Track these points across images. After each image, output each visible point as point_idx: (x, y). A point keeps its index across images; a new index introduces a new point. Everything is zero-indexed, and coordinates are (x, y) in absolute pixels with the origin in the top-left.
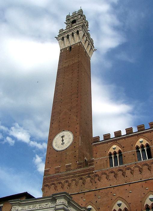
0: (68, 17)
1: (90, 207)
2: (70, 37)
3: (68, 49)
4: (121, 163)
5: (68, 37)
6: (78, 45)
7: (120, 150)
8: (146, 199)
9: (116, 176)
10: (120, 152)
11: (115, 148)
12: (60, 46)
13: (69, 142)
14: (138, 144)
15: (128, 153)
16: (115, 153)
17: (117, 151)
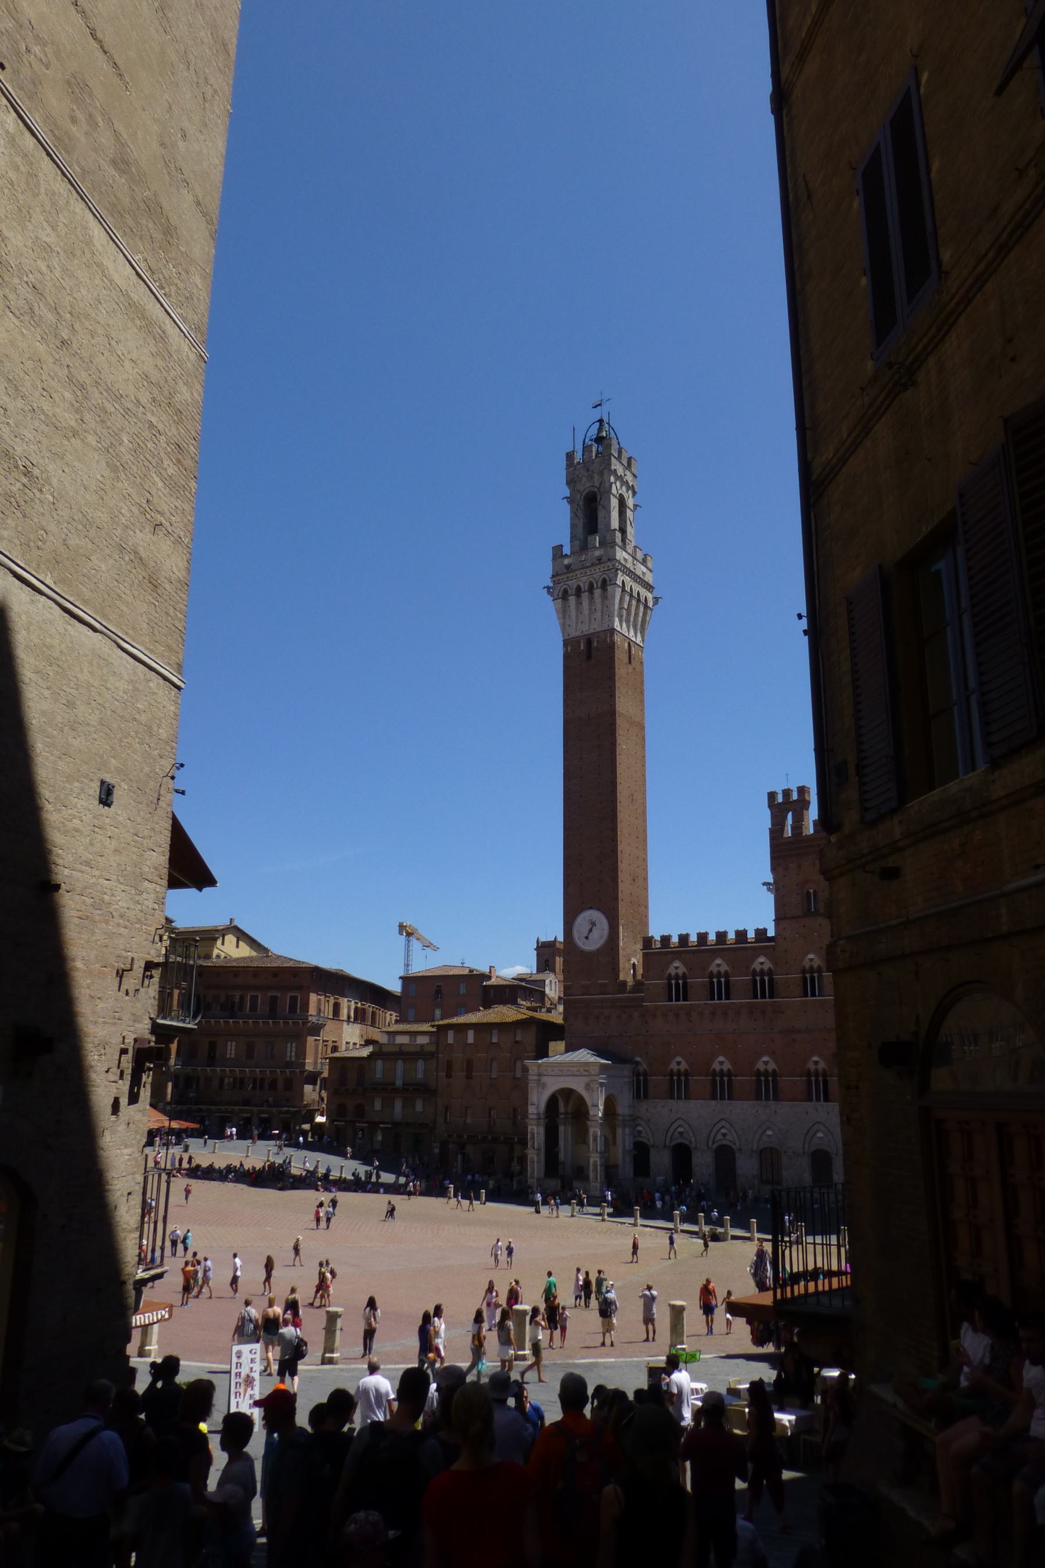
0: (570, 456)
1: (638, 1059)
2: (585, 596)
3: (582, 648)
4: (687, 1000)
5: (579, 592)
6: (608, 639)
7: (684, 972)
8: (713, 1061)
9: (677, 1016)
10: (684, 977)
11: (677, 967)
12: (563, 627)
13: (601, 937)
14: (713, 968)
15: (698, 981)
16: (677, 977)
17: (680, 972)
